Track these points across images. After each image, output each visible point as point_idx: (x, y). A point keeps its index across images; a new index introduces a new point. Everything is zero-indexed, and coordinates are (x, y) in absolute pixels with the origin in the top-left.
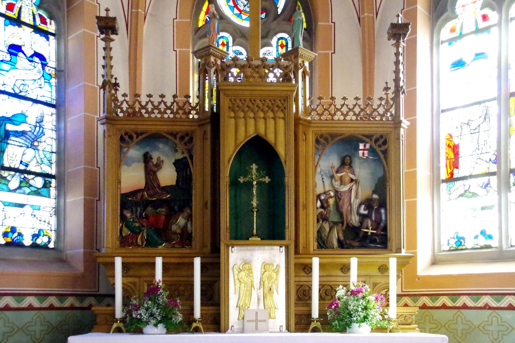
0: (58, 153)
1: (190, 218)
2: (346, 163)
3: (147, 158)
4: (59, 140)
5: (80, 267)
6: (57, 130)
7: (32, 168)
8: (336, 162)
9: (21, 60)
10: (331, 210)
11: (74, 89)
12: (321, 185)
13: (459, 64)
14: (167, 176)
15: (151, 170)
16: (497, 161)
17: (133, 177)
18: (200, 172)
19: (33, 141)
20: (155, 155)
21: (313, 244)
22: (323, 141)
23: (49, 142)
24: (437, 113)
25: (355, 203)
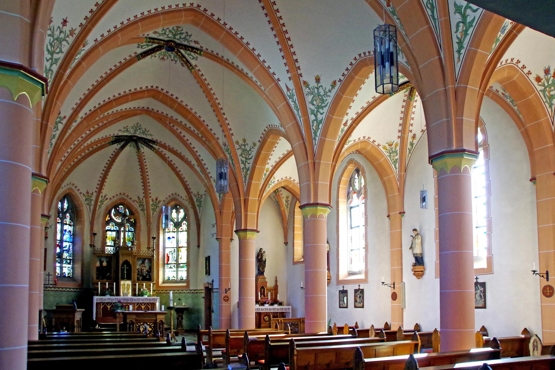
0: (73, 254)
1: (111, 273)
2: (143, 263)
3: (100, 260)
4: (73, 251)
5: (80, 282)
6: (73, 248)
7: (68, 258)
8: (140, 262)
9: (67, 233)
10: (140, 273)
11: (77, 239)
12: (138, 267)
13: (169, 238)
14: (105, 264)
15: (101, 262)
16: (176, 261)
17: (98, 264)
18: (113, 264)
19: (68, 251)
20: (102, 259)
21: (136, 280)
22: (139, 259)
23: (71, 252)
24: (164, 248)
25: (145, 271)
